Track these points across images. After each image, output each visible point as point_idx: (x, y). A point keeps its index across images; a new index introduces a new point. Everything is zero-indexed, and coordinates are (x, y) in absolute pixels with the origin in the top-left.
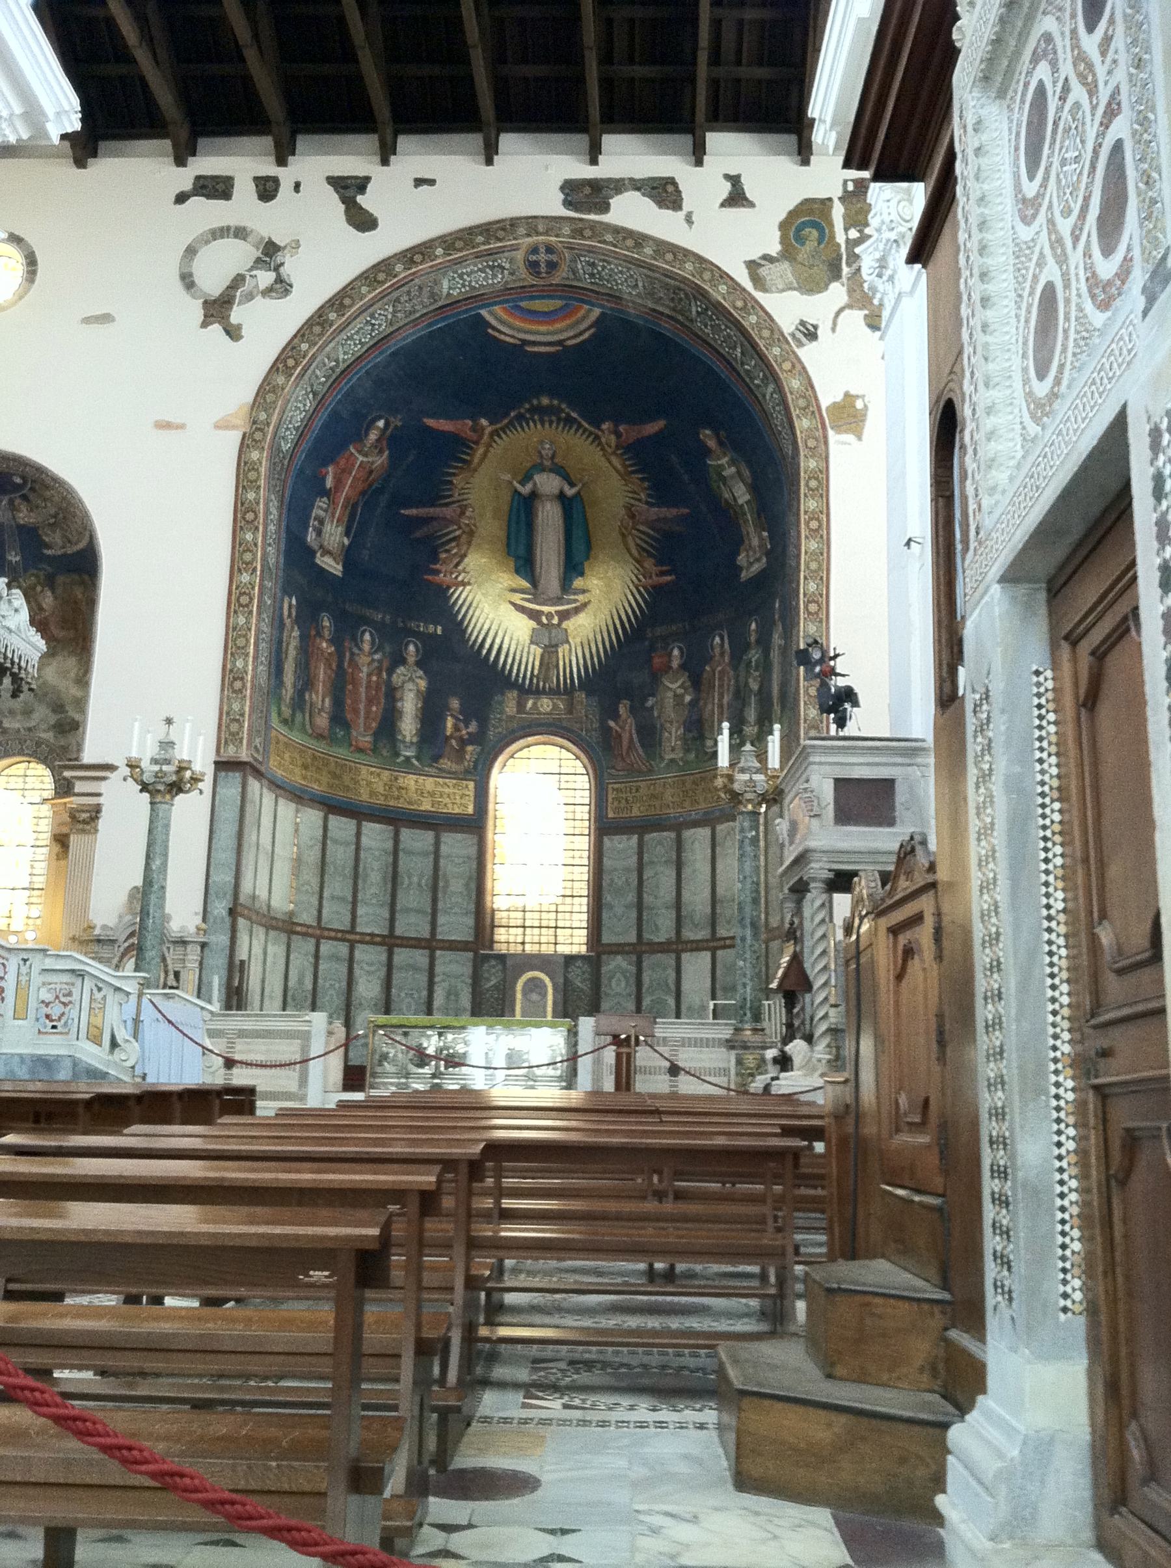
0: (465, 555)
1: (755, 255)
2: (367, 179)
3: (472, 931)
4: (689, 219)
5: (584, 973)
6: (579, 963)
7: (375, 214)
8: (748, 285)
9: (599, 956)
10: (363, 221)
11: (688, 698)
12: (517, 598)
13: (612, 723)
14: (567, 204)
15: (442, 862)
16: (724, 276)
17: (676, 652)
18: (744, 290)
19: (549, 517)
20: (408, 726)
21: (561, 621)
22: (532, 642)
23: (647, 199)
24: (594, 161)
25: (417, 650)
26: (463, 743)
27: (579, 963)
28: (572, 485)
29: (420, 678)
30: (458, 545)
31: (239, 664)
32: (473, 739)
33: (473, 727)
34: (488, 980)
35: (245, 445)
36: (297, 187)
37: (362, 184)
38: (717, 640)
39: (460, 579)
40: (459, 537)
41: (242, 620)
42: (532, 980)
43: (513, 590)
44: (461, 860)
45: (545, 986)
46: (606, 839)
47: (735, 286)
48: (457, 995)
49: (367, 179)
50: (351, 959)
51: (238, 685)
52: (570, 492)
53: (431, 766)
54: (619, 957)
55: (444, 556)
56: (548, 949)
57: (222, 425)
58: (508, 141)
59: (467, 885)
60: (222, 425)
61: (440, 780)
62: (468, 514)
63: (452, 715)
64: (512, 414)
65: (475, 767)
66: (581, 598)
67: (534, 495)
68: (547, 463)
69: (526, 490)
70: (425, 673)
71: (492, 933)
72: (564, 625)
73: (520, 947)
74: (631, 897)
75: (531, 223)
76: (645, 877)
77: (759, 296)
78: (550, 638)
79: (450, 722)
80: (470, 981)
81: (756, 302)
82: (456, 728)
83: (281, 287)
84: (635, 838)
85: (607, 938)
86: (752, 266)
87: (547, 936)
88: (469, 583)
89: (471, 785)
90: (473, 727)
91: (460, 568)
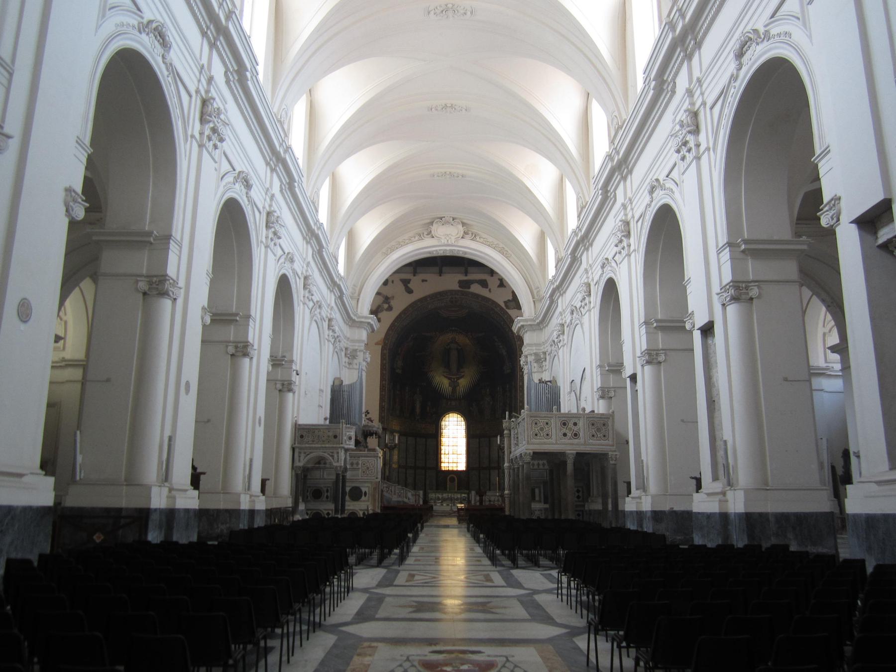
1: (506, 300)
2: (410, 280)
4: (490, 291)
7: (413, 289)
8: (504, 308)
10: (410, 291)
11: (491, 403)
12: (445, 374)
14: (460, 287)
16: (499, 305)
17: (488, 390)
18: (503, 308)
20: (418, 410)
21: (457, 380)
22: (449, 386)
23: (479, 285)
24: (466, 275)
31: (384, 404)
35: (382, 350)
36: (393, 282)
37: (409, 281)
38: (498, 388)
41: (384, 393)
42: (450, 478)
43: (444, 372)
45: (455, 480)
47: (501, 308)
49: (410, 280)
50: (406, 473)
51: (383, 409)
56: (455, 469)
57: (377, 344)
58: (444, 269)
60: (377, 344)
66: (462, 374)
69: (449, 347)
71: (441, 465)
72: (458, 381)
75: (451, 292)
77: (507, 310)
79: (428, 408)
81: (506, 312)
83: (390, 309)
86: (505, 303)
87: (455, 465)
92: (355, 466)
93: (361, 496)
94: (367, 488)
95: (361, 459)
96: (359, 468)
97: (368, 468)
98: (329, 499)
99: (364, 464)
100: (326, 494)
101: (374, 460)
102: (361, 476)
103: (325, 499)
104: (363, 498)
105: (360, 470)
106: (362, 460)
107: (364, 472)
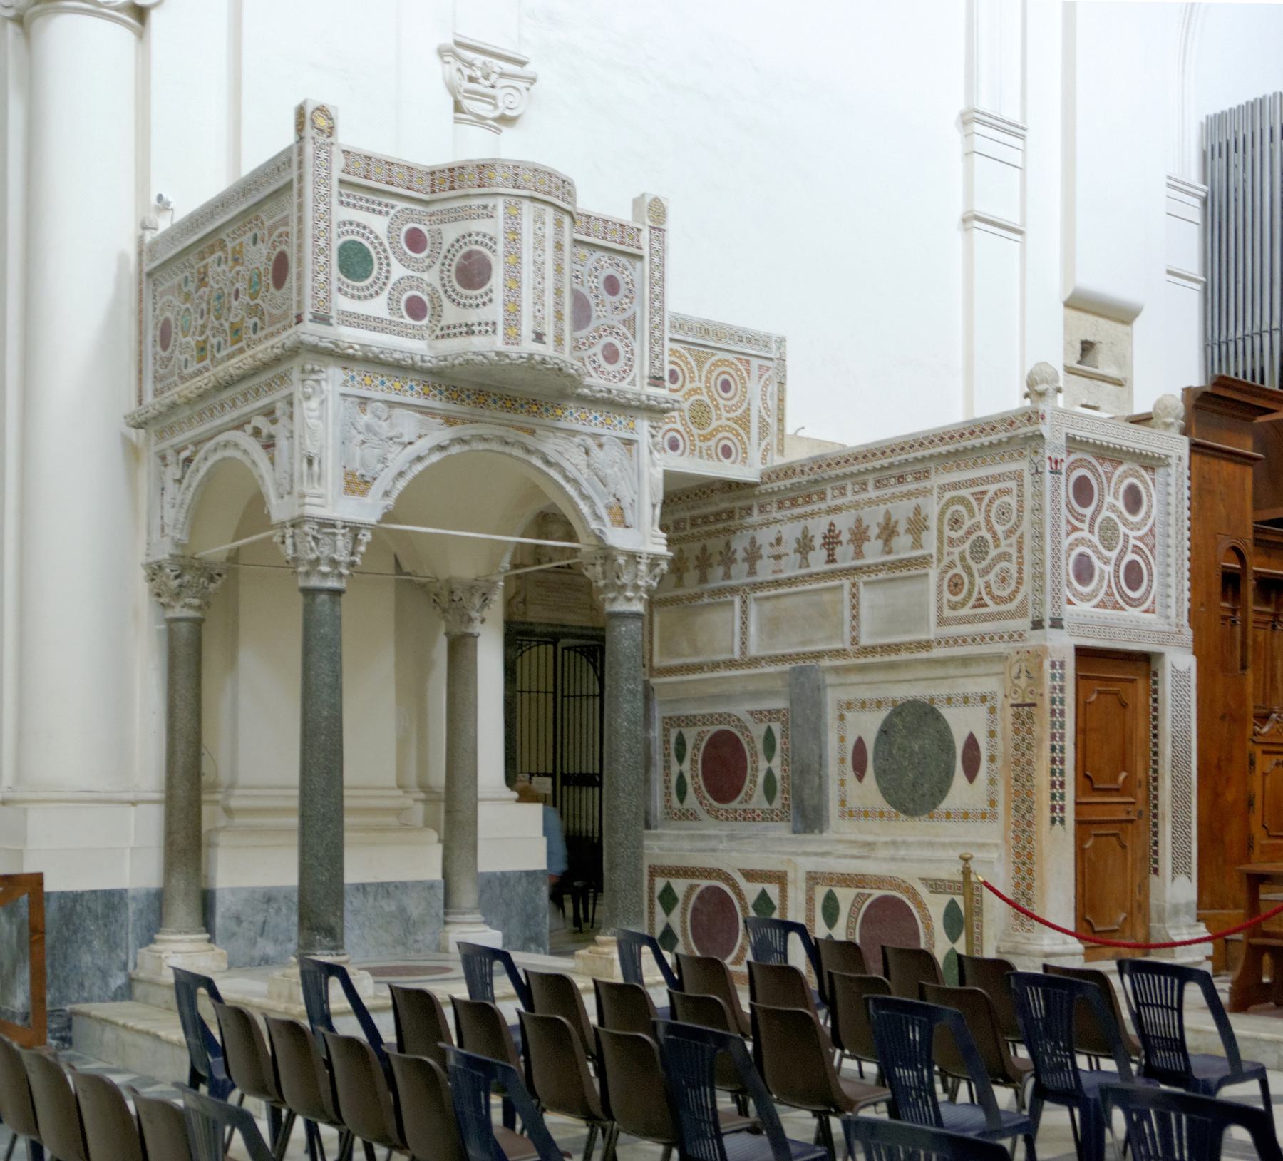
92: (903, 547)
93: (948, 774)
94: (982, 711)
95: (939, 479)
96: (923, 561)
97: (980, 549)
98: (777, 803)
99: (956, 522)
100: (763, 765)
101: (1018, 476)
102: (942, 622)
103: (758, 800)
104: (961, 792)
105: (933, 573)
106: (944, 488)
107: (955, 586)
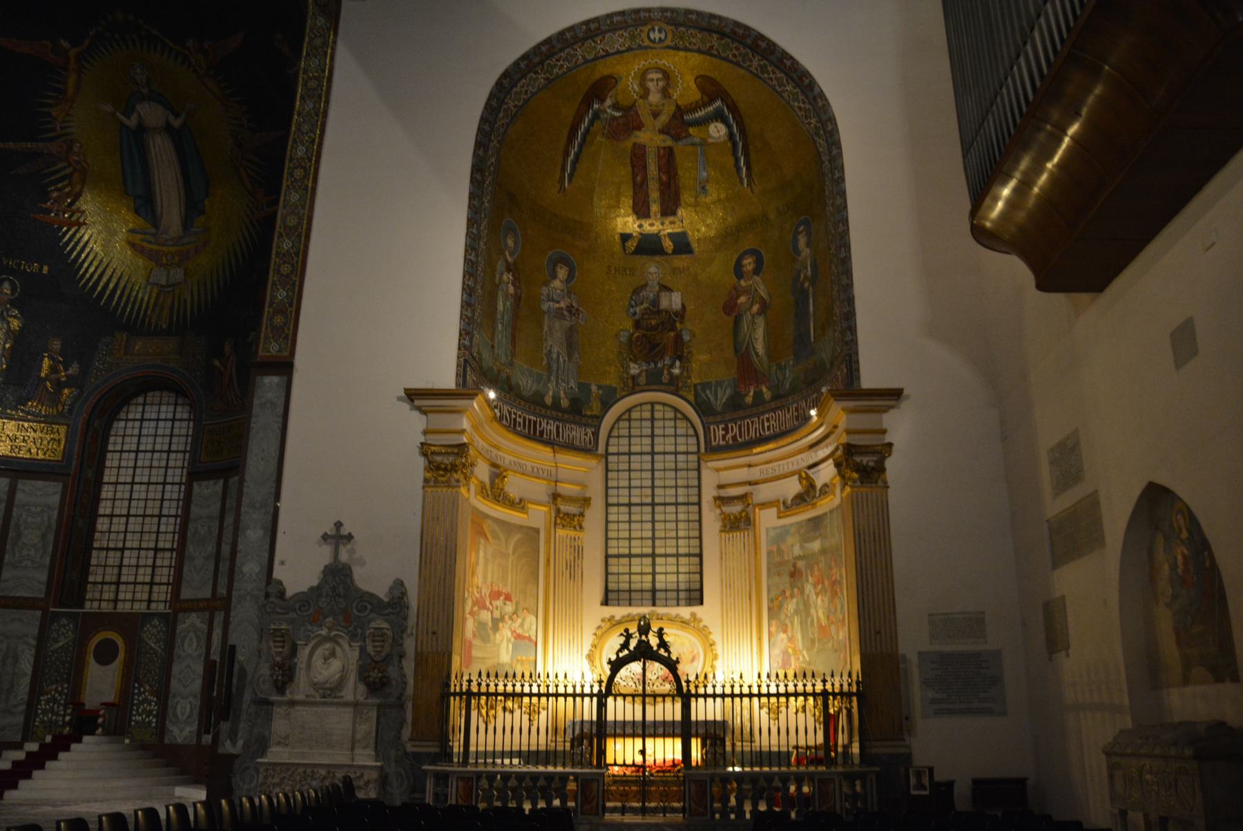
0: (77, 197)
3: (43, 588)
5: (159, 632)
6: (156, 622)
9: (176, 613)
12: (137, 238)
13: (217, 363)
15: (15, 512)
19: (161, 150)
25: (14, 289)
26: (59, 386)
27: (156, 622)
28: (177, 115)
29: (14, 317)
30: (70, 184)
32: (71, 382)
33: (74, 369)
34: (56, 641)
39: (74, 218)
40: (71, 174)
44: (39, 509)
46: (195, 484)
48: (16, 659)
52: (177, 123)
53: (16, 409)
54: (194, 615)
55: (55, 194)
59: (44, 536)
61: (26, 425)
62: (76, 149)
63: (50, 357)
64: (91, 33)
65: (70, 411)
67: (141, 129)
68: (145, 91)
69: (132, 122)
70: (21, 312)
73: (111, 605)
74: (211, 548)
76: (225, 525)
78: (168, 281)
79: (46, 363)
80: (34, 642)
82: (53, 369)
84: (221, 482)
85: (186, 594)
88: (84, 223)
89: (63, 429)
90: (74, 369)
91: (74, 207)
